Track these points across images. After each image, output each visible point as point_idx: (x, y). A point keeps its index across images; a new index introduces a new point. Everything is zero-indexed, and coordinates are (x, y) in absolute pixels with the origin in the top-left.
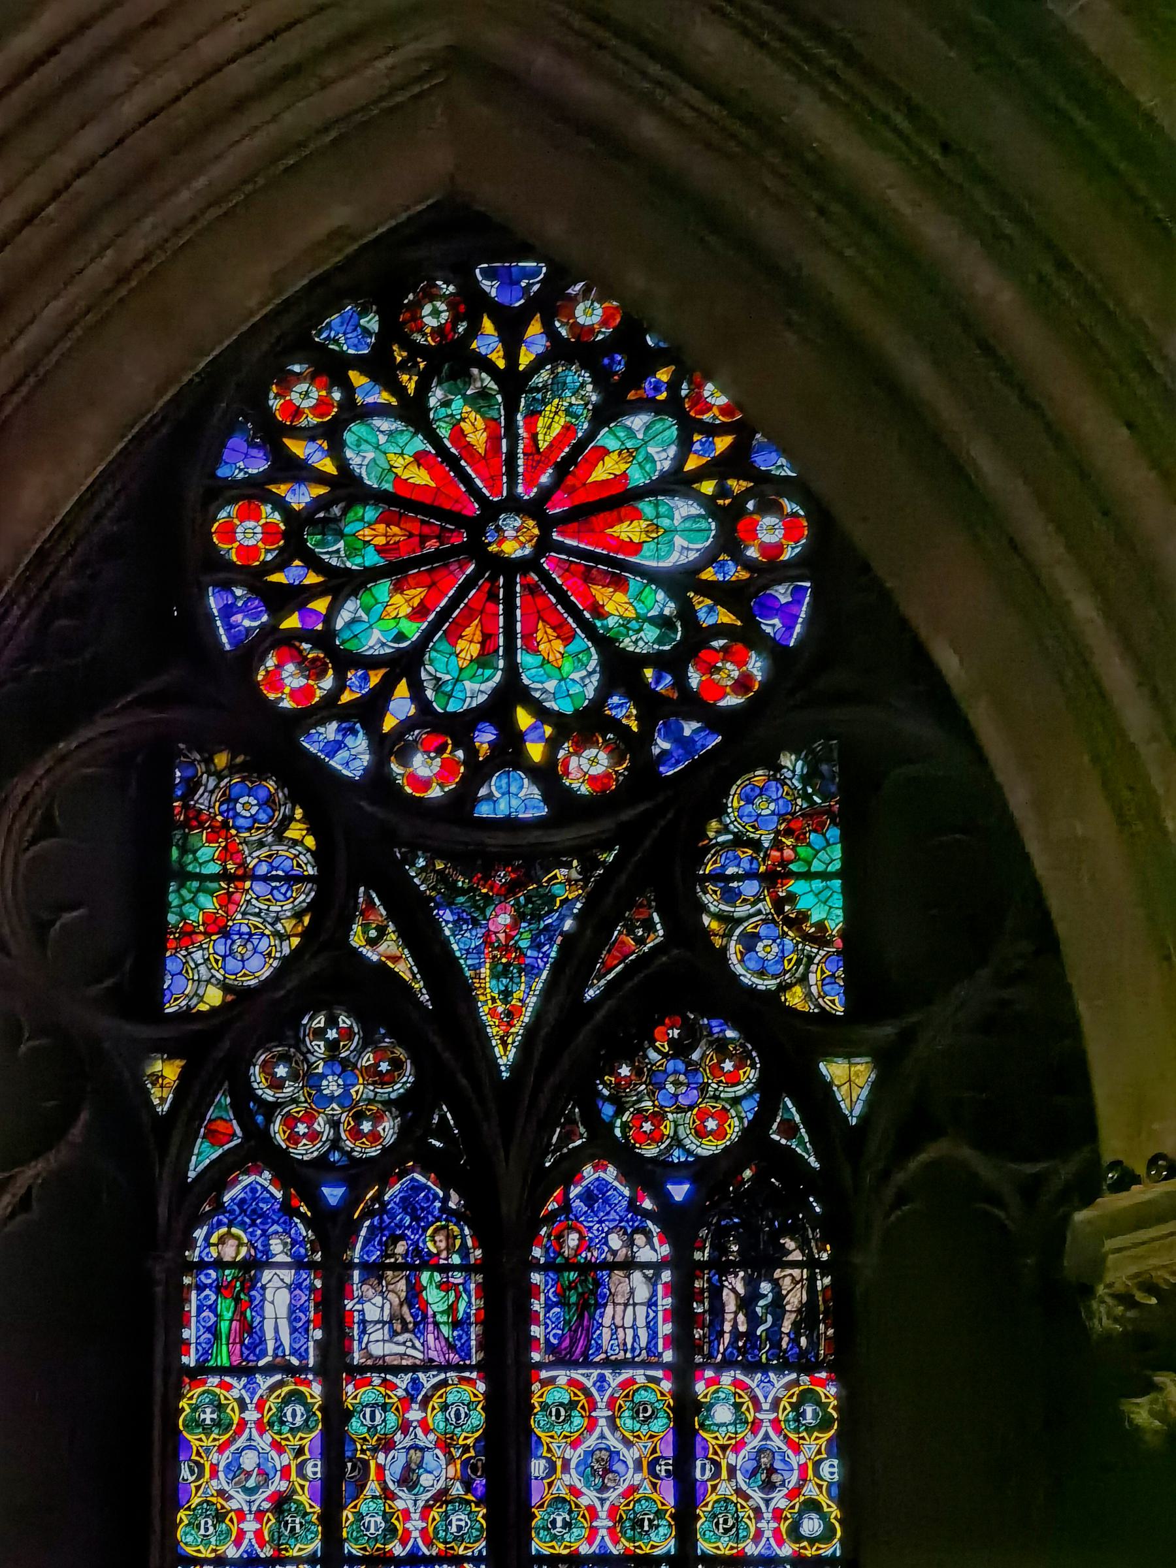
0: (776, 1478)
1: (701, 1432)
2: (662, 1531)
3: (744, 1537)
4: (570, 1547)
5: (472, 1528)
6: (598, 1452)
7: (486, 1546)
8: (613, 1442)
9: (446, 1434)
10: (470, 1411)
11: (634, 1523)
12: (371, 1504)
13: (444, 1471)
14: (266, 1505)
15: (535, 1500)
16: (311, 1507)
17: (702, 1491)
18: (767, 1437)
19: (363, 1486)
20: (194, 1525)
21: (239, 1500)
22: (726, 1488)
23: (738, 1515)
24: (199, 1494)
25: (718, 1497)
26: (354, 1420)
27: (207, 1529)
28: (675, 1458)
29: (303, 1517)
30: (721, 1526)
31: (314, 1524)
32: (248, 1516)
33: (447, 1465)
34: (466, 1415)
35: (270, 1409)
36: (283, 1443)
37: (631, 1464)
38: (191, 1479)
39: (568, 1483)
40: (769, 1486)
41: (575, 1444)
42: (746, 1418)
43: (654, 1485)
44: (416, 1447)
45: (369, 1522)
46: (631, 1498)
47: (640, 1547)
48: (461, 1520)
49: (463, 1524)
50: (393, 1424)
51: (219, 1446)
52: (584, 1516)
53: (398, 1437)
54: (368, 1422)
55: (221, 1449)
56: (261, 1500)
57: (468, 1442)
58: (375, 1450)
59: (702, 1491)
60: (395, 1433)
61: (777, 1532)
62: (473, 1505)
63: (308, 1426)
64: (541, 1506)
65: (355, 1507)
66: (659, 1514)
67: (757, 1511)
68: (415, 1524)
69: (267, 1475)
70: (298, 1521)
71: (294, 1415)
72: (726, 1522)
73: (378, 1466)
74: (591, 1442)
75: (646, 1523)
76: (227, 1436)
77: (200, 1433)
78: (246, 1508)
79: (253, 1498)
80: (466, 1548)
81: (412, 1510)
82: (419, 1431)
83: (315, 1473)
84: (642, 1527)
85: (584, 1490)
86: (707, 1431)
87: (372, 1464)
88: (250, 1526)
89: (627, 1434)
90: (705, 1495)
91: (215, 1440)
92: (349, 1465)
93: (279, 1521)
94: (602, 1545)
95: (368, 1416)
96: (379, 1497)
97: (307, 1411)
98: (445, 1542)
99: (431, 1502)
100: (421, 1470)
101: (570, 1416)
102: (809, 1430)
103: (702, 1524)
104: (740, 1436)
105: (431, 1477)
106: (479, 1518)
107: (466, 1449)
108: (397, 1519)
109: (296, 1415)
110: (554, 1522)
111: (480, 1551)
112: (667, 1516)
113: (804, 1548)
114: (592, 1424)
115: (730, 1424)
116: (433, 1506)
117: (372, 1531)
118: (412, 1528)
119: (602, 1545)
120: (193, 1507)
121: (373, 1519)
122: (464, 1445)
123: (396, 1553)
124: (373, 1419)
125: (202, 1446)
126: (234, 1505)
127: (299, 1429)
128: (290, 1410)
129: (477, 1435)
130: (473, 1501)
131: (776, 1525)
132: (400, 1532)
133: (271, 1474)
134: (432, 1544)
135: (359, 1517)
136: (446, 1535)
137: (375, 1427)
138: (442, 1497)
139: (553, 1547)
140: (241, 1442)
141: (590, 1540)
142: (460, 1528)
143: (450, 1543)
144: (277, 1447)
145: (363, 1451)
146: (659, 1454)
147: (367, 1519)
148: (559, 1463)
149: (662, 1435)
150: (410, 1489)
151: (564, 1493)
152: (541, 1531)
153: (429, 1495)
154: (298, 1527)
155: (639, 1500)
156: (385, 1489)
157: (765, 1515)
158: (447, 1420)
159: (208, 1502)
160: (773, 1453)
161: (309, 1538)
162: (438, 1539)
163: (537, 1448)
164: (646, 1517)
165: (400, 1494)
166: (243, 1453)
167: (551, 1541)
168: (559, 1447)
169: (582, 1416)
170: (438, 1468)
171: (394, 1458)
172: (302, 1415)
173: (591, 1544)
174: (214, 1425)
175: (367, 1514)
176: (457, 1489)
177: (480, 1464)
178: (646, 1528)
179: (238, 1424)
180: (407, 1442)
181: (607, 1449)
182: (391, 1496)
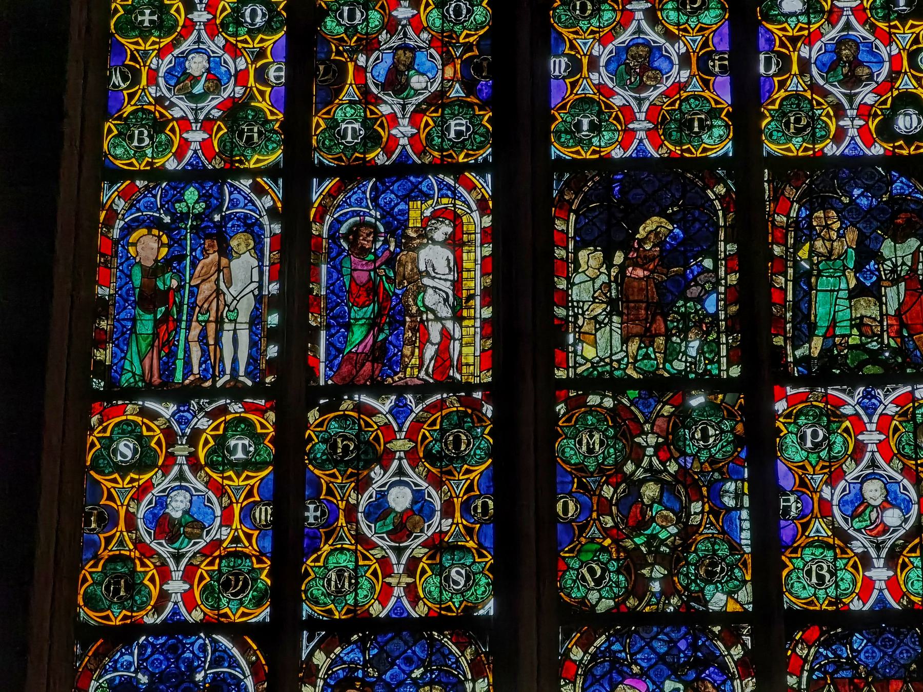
0: (860, 71)
1: (764, 23)
2: (717, 132)
3: (822, 137)
4: (600, 152)
5: (475, 133)
6: (634, 48)
7: (493, 154)
8: (653, 36)
9: (443, 31)
10: (472, 5)
11: (681, 124)
12: (348, 109)
13: (440, 72)
14: (216, 113)
15: (555, 101)
16: (272, 113)
17: (767, 87)
18: (848, 26)
19: (341, 90)
20: (125, 135)
21: (181, 108)
22: (795, 84)
23: (814, 113)
24: (133, 103)
25: (787, 93)
26: (328, 19)
27: (141, 140)
28: (731, 53)
29: (263, 125)
30: (792, 126)
31: (276, 132)
32: (194, 125)
33: (444, 65)
34: (468, 11)
35: (224, 9)
36: (240, 45)
37: (675, 59)
38: (123, 86)
39: (596, 82)
40: (852, 81)
41: (604, 42)
42: (822, 6)
43: (706, 83)
44: (405, 47)
45: (346, 129)
46: (678, 96)
47: (689, 151)
48: (461, 125)
49: (464, 128)
50: (377, 23)
51: (159, 50)
52: (617, 118)
53: (383, 36)
54: (346, 21)
55: (161, 54)
56: (211, 106)
57: (471, 39)
58: (354, 51)
59: (767, 87)
60: (379, 32)
61: (863, 131)
62: (476, 108)
63: (271, 27)
64: (563, 107)
65: (328, 113)
66: (714, 113)
67: (839, 111)
68: (404, 130)
69: (219, 80)
70: (256, 130)
71: (254, 14)
72: (797, 121)
73: (357, 68)
74: (625, 37)
75: (696, 124)
76: (169, 39)
77: (136, 37)
78: (191, 117)
79: (200, 105)
80: (467, 156)
81: (399, 115)
82: (410, 30)
83: (278, 78)
84: (691, 128)
85: (617, 89)
86: (772, 22)
87: (351, 66)
88: (196, 136)
89: (671, 28)
90: (771, 91)
91: (154, 43)
92: (321, 68)
93: (231, 130)
94: (640, 149)
95: (346, 14)
96: (360, 102)
97: (270, 11)
98: (441, 150)
99: (424, 106)
100: (412, 72)
101: (599, 10)
102: (903, 19)
103: (769, 123)
104: (814, 27)
105: (423, 79)
106: (484, 122)
107: (468, 47)
108: (382, 125)
109: (257, 15)
110: (578, 126)
111: (485, 159)
112: (722, 116)
113: (900, 147)
114: (627, 18)
115: (802, 14)
116: (426, 110)
117: (349, 139)
118: (400, 135)
119: (640, 149)
120: (125, 115)
121: (350, 126)
122: (464, 44)
123: (379, 162)
124: (352, 16)
125: (138, 51)
126: (177, 113)
127: (259, 30)
128: (249, 11)
129: (482, 32)
130: (477, 104)
131: (862, 123)
132: (384, 140)
133: (225, 79)
134: (424, 152)
135: (333, 124)
136: (443, 141)
137: (355, 27)
138: (438, 100)
139: (578, 152)
140: (185, 46)
141: (624, 145)
142: (459, 134)
143: (447, 150)
144: (233, 50)
145: (339, 53)
146: (712, 48)
147: (344, 126)
148: (585, 61)
149: (715, 27)
150: (397, 93)
151: (590, 92)
152: (563, 135)
153: (421, 98)
154: (256, 135)
155: (687, 99)
156: (365, 91)
157: (849, 113)
158: (444, 17)
159: (143, 110)
160: (857, 45)
161: (270, 148)
162: (432, 147)
163: (558, 46)
164: (696, 117)
165: (385, 98)
166: (190, 57)
167: (576, 146)
168: (585, 44)
169: (614, 10)
170: (433, 68)
171: (377, 58)
172: (264, 15)
173: (625, 149)
174: (153, 28)
175: (343, 121)
176: (457, 92)
177: (485, 64)
178: (696, 129)
179: (183, 27)
180: (395, 42)
181: (646, 44)
182: (373, 101)
